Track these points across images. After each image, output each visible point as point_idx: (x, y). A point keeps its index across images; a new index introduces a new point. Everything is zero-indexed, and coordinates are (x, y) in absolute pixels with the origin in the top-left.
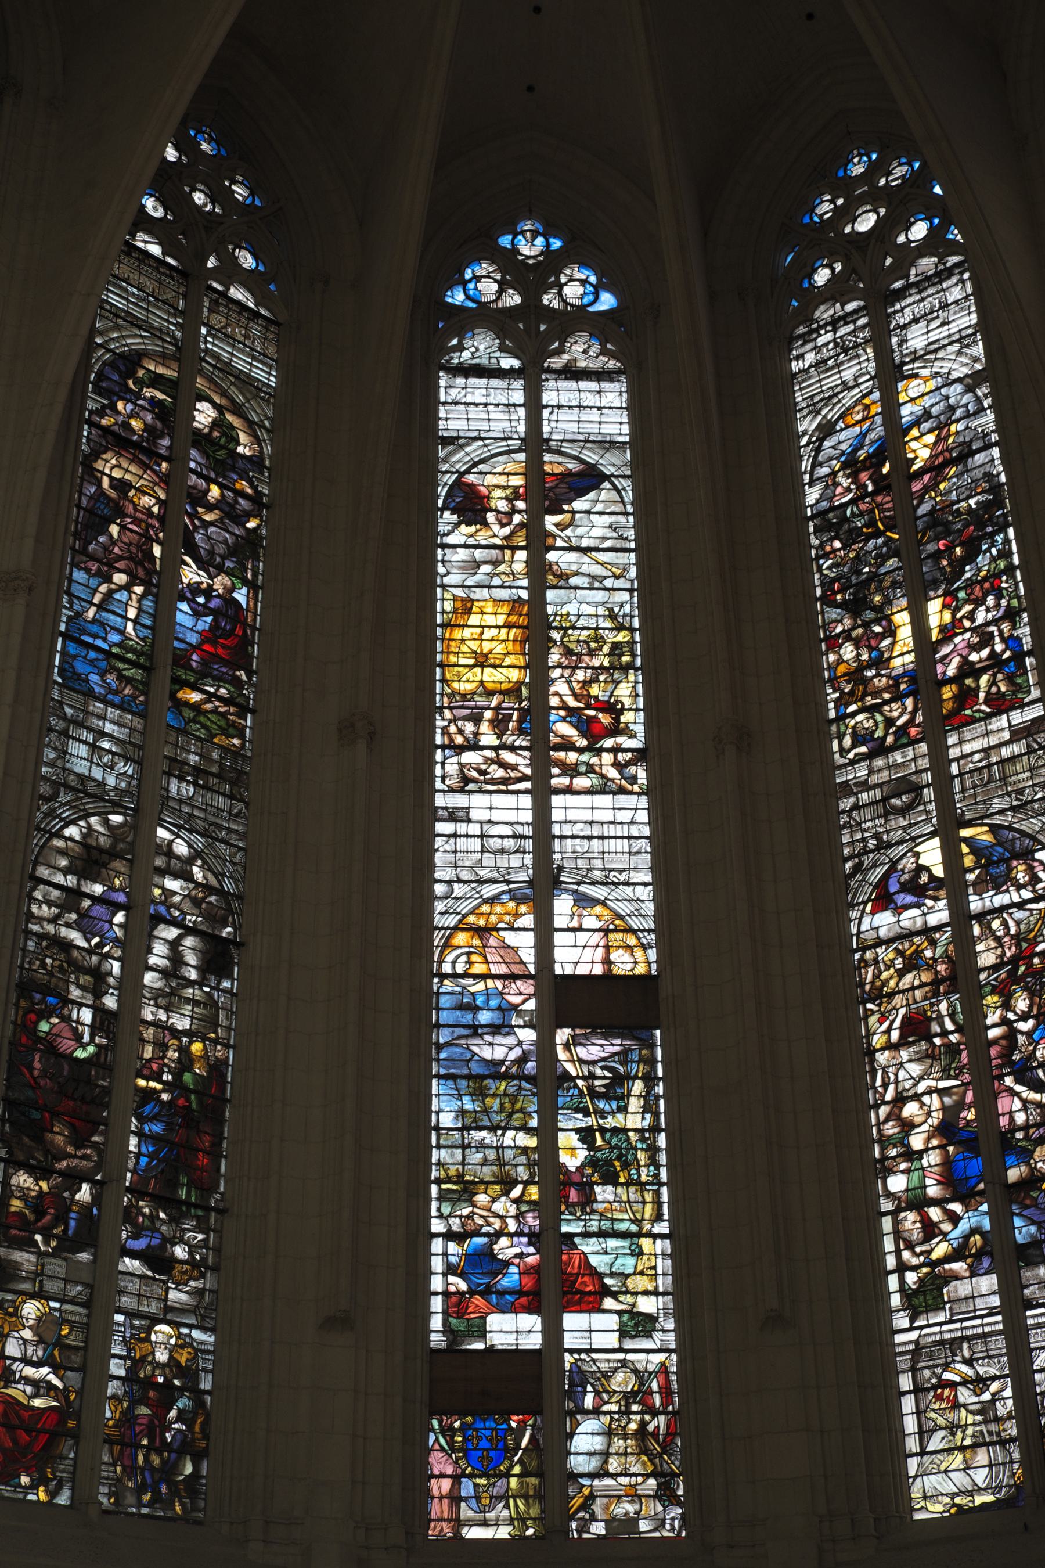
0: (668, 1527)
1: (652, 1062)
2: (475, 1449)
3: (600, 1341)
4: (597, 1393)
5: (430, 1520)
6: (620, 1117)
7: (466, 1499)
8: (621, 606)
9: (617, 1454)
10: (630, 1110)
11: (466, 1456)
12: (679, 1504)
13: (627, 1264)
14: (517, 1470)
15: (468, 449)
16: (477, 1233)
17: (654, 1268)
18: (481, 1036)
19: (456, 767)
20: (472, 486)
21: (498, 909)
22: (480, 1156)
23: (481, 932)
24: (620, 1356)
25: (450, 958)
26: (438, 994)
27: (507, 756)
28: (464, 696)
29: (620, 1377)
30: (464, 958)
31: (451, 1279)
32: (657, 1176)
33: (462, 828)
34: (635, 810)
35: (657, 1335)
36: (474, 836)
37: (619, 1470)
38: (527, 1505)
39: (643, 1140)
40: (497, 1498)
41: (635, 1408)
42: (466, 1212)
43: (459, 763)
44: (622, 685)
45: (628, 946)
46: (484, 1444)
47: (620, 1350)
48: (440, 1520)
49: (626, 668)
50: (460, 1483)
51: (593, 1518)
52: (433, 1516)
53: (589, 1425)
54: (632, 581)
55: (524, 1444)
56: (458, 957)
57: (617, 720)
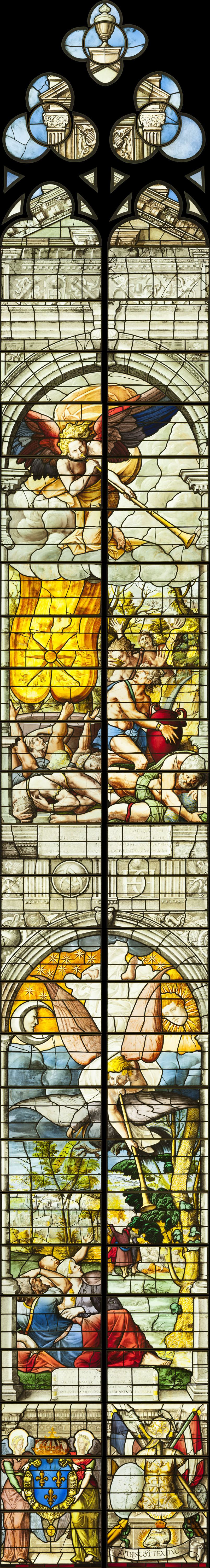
0: (192, 1554)
1: (199, 1122)
3: (140, 1393)
6: (166, 1177)
8: (190, 586)
10: (176, 1171)
12: (202, 1536)
13: (167, 1321)
15: (35, 367)
16: (42, 1294)
17: (192, 1326)
18: (48, 1097)
19: (24, 793)
20: (39, 422)
21: (64, 958)
22: (47, 1218)
23: (51, 982)
24: (158, 1407)
25: (18, 1013)
26: (7, 1052)
27: (76, 779)
28: (31, 706)
29: (157, 1424)
30: (32, 1013)
31: (20, 1337)
32: (198, 1236)
33: (31, 866)
34: (192, 841)
35: (191, 1389)
36: (42, 875)
39: (187, 1201)
41: (169, 1452)
42: (32, 1274)
43: (27, 789)
44: (186, 688)
45: (182, 999)
47: (159, 1402)
49: (191, 667)
53: (128, 1468)
54: (202, 550)
56: (27, 1011)
57: (179, 732)
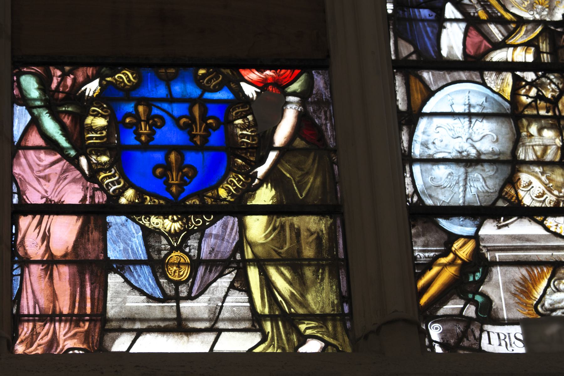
2: (145, 147)
4: (472, 23)
5: (19, 319)
7: (121, 267)
9: (539, 162)
11: (122, 159)
14: (265, 196)
37: (550, 200)
38: (299, 281)
40: (210, 264)
46: (169, 135)
48: (50, 317)
50: (104, 228)
51: (488, 315)
52: (27, 306)
55: (282, 135)
